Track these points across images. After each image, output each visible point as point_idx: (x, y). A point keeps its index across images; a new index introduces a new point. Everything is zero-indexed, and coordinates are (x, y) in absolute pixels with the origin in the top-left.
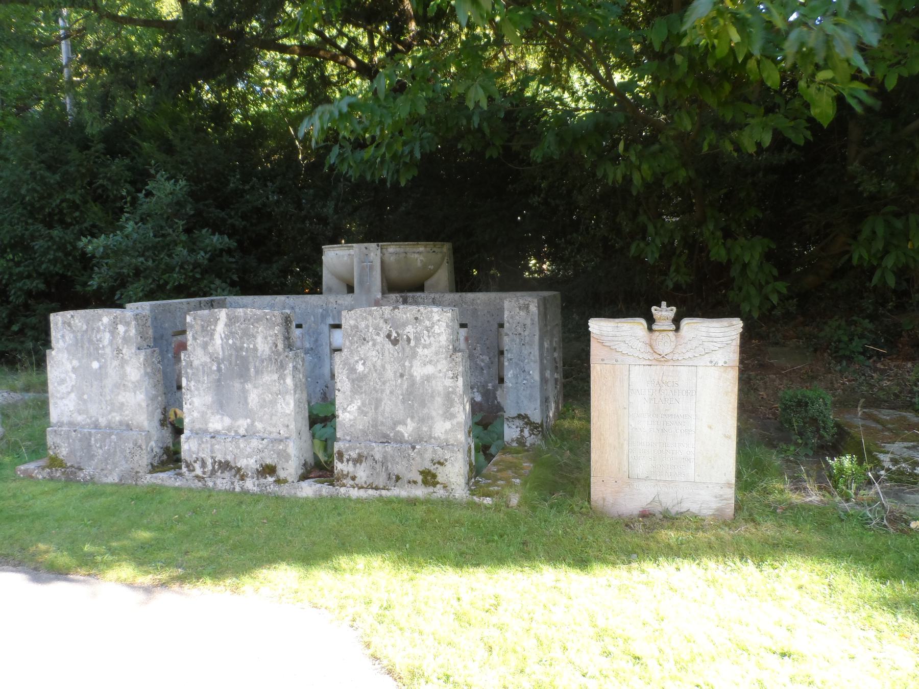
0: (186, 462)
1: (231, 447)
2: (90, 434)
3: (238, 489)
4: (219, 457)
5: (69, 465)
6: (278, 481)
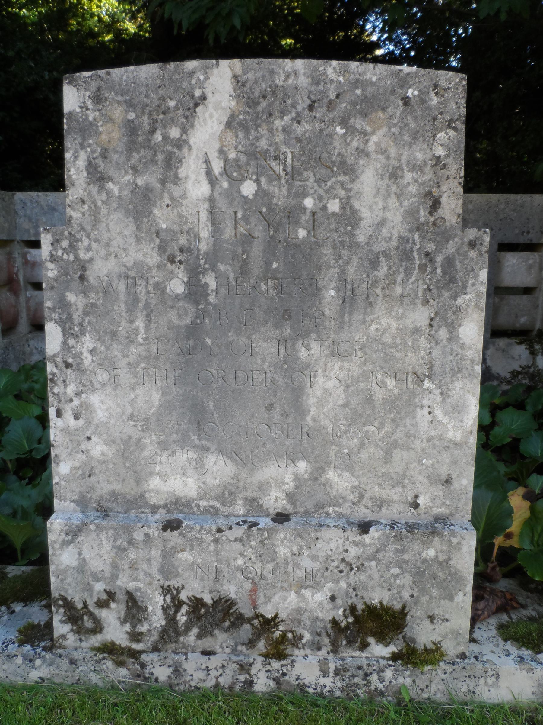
0: (68, 605)
1: (238, 554)
3: (262, 684)
4: (194, 587)
6: (411, 657)
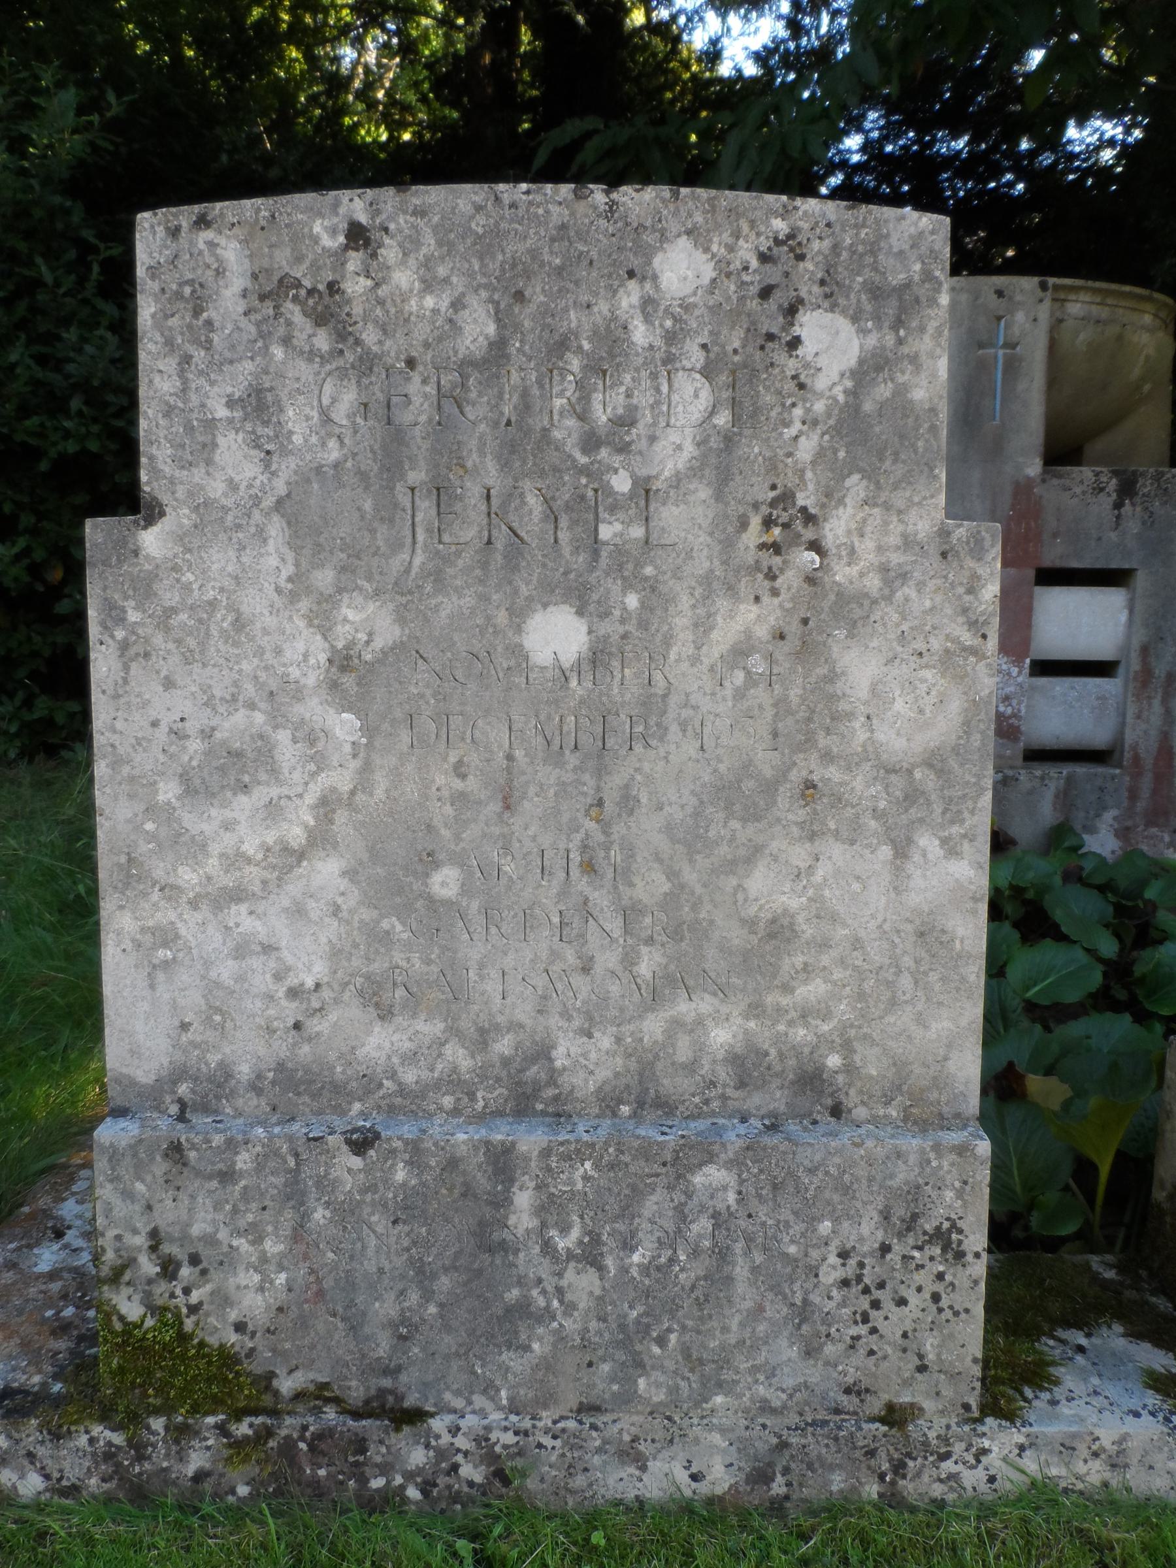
2: (503, 1163)
5: (286, 1385)
